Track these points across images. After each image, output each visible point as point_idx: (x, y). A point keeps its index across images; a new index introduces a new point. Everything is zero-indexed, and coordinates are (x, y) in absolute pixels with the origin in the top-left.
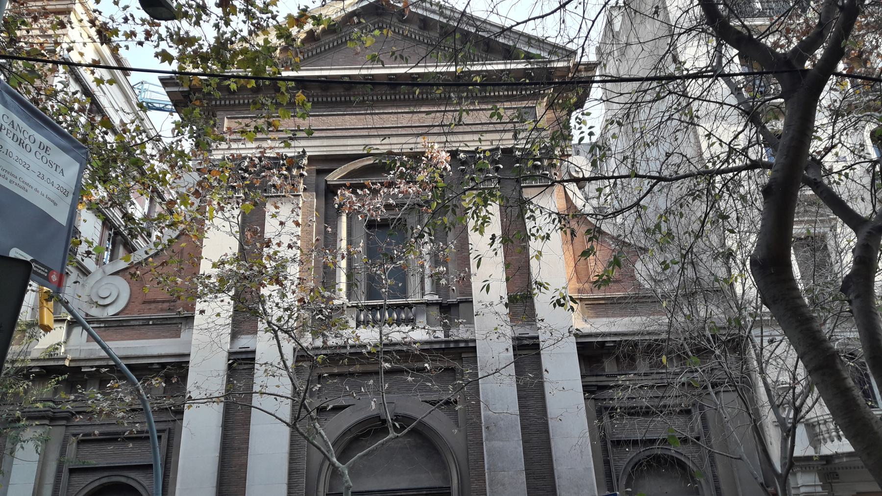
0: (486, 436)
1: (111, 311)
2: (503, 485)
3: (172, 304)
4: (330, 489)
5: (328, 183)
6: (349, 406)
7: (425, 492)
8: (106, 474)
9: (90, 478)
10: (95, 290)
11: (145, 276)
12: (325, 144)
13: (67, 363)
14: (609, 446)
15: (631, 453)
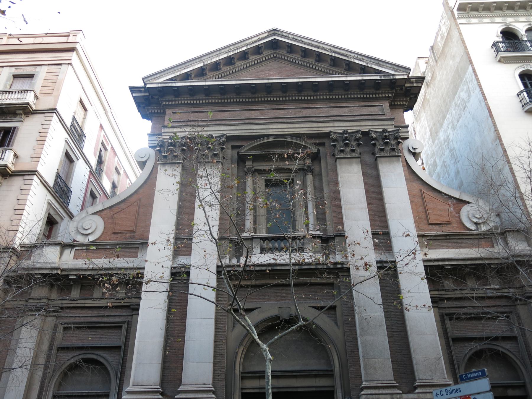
0: (360, 333)
1: (91, 238)
2: (375, 369)
3: (133, 234)
4: (244, 368)
5: (240, 154)
6: (256, 308)
7: (314, 373)
8: (83, 352)
9: (71, 354)
10: (80, 224)
11: (115, 215)
12: (238, 128)
13: (59, 272)
14: (451, 342)
15: (475, 346)
